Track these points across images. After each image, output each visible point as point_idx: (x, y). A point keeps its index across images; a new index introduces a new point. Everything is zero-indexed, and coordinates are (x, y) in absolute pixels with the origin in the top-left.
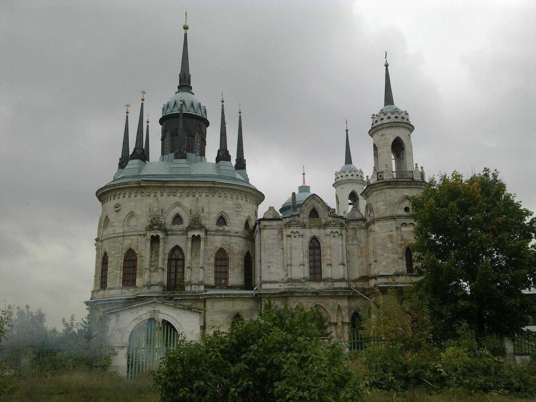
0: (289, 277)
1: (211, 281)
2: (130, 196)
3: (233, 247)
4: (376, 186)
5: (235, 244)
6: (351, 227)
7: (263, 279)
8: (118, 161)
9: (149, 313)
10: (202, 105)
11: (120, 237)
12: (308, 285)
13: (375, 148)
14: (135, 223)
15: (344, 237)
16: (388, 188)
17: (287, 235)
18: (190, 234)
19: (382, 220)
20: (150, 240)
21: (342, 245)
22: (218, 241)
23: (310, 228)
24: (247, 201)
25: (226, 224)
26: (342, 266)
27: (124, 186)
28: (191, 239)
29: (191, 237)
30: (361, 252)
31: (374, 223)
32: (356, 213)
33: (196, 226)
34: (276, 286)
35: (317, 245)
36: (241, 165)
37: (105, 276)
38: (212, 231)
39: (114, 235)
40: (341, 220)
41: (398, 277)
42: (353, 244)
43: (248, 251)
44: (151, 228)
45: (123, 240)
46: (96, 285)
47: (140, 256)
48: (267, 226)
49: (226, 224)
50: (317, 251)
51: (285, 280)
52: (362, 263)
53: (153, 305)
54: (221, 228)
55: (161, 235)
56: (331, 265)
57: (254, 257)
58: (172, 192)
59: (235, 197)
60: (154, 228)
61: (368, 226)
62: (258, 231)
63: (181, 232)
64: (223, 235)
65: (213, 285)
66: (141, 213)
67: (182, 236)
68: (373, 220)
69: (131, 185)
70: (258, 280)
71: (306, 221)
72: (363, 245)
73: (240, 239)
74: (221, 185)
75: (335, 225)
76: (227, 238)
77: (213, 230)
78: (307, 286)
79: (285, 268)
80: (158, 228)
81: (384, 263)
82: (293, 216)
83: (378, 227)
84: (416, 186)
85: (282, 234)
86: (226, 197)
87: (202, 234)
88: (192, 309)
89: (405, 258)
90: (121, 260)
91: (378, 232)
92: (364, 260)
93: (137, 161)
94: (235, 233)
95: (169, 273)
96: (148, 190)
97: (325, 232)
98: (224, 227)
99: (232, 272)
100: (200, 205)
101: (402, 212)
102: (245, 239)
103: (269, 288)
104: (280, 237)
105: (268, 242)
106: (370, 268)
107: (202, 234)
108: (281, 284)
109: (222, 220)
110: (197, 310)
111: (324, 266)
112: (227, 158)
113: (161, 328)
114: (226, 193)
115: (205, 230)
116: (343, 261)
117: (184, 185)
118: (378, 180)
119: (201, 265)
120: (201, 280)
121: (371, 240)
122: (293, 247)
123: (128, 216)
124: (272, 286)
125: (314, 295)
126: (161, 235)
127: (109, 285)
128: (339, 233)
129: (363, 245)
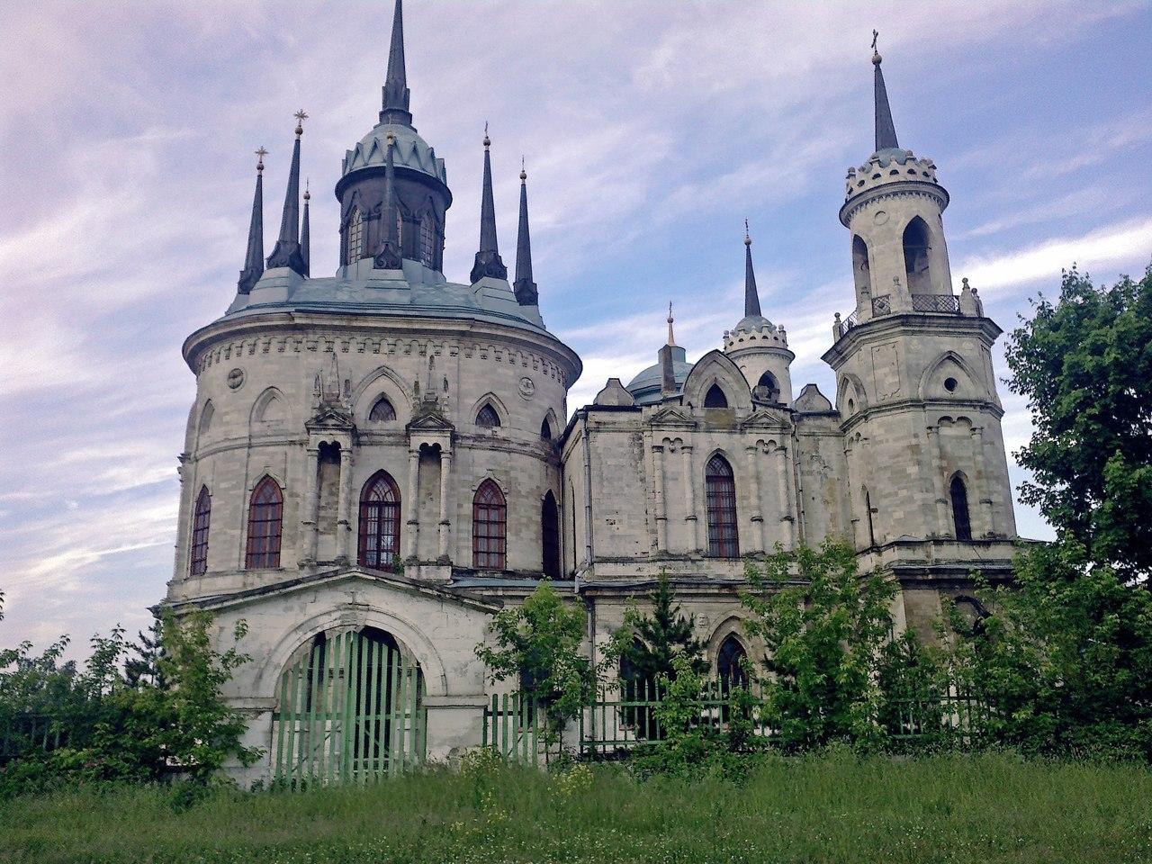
0: (661, 547)
1: (466, 560)
2: (266, 350)
3: (516, 478)
4: (871, 328)
5: (522, 470)
6: (806, 430)
7: (597, 552)
8: (238, 278)
9: (338, 609)
10: (437, 156)
11: (241, 447)
12: (708, 568)
13: (860, 245)
14: (280, 416)
15: (790, 455)
16: (905, 332)
17: (653, 447)
18: (417, 440)
19: (890, 410)
20: (317, 454)
21: (786, 472)
22: (481, 463)
23: (709, 430)
24: (545, 372)
25: (498, 423)
26: (787, 523)
27: (253, 325)
28: (417, 452)
29: (418, 449)
30: (831, 493)
31: (866, 417)
32: (815, 399)
33: (431, 423)
34: (630, 570)
35: (724, 472)
36: (527, 292)
37: (202, 545)
38: (468, 438)
39: (228, 444)
40: (780, 414)
41: (939, 548)
42: (810, 473)
43: (550, 491)
44: (319, 422)
45: (249, 456)
46: (179, 566)
47: (291, 496)
48: (605, 423)
49: (498, 423)
50: (725, 488)
51: (650, 554)
52: (833, 518)
53: (351, 587)
54: (488, 433)
55: (345, 441)
56: (760, 520)
57: (563, 506)
58: (369, 342)
59: (519, 360)
60: (327, 425)
61: (845, 428)
62: (584, 435)
63: (391, 439)
64: (493, 449)
65: (471, 567)
66: (294, 391)
67: (394, 447)
68: (865, 411)
69: (269, 323)
70: (582, 554)
71: (700, 412)
72: (834, 475)
73: (536, 461)
74: (487, 328)
75: (768, 424)
76: (501, 456)
77: (468, 435)
78: (706, 571)
79: (649, 527)
80: (338, 426)
81: (899, 514)
82: (666, 400)
83: (880, 426)
84: (970, 331)
85: (642, 445)
86: (498, 359)
87: (445, 443)
88: (465, 601)
89: (950, 503)
90: (244, 502)
91: (878, 439)
92: (839, 510)
93: (285, 271)
94: (520, 444)
95: (363, 537)
96: (311, 337)
97: (743, 441)
98: (495, 429)
99: (514, 538)
100: (439, 374)
101: (940, 391)
102: (544, 463)
103: (614, 574)
104: (636, 450)
105: (609, 463)
106: (854, 529)
107: (445, 443)
108: (640, 565)
109: (489, 414)
110: (478, 604)
111: (742, 521)
112: (500, 272)
113: (342, 672)
114: (498, 348)
115: (452, 432)
116: (789, 513)
117: (399, 326)
119: (442, 518)
120: (442, 552)
121: (854, 459)
122: (668, 475)
123: (261, 399)
124: (619, 570)
125: (725, 591)
126: (345, 441)
127: (212, 566)
128: (779, 445)
129: (834, 475)
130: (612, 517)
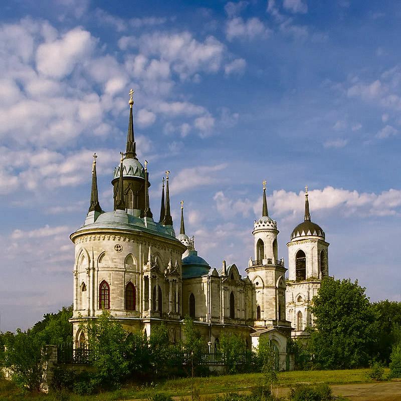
71: (230, 281)
72: (250, 300)
106: (253, 314)
111: (235, 310)
118: (268, 263)
129: (250, 300)
130: (214, 306)
